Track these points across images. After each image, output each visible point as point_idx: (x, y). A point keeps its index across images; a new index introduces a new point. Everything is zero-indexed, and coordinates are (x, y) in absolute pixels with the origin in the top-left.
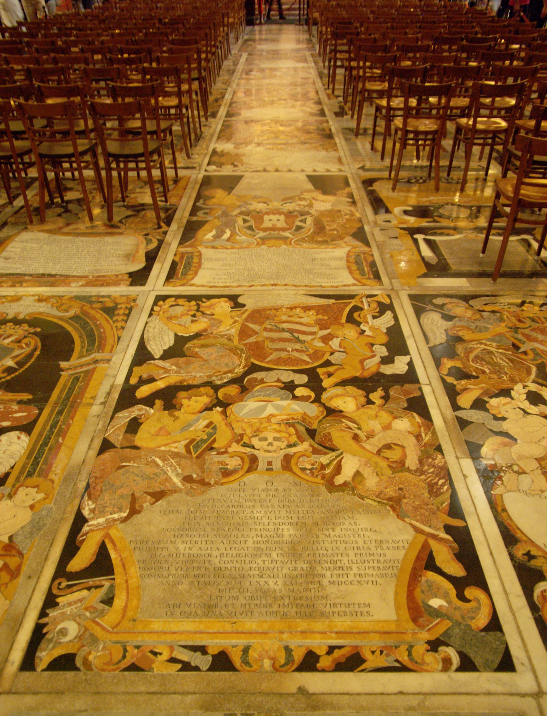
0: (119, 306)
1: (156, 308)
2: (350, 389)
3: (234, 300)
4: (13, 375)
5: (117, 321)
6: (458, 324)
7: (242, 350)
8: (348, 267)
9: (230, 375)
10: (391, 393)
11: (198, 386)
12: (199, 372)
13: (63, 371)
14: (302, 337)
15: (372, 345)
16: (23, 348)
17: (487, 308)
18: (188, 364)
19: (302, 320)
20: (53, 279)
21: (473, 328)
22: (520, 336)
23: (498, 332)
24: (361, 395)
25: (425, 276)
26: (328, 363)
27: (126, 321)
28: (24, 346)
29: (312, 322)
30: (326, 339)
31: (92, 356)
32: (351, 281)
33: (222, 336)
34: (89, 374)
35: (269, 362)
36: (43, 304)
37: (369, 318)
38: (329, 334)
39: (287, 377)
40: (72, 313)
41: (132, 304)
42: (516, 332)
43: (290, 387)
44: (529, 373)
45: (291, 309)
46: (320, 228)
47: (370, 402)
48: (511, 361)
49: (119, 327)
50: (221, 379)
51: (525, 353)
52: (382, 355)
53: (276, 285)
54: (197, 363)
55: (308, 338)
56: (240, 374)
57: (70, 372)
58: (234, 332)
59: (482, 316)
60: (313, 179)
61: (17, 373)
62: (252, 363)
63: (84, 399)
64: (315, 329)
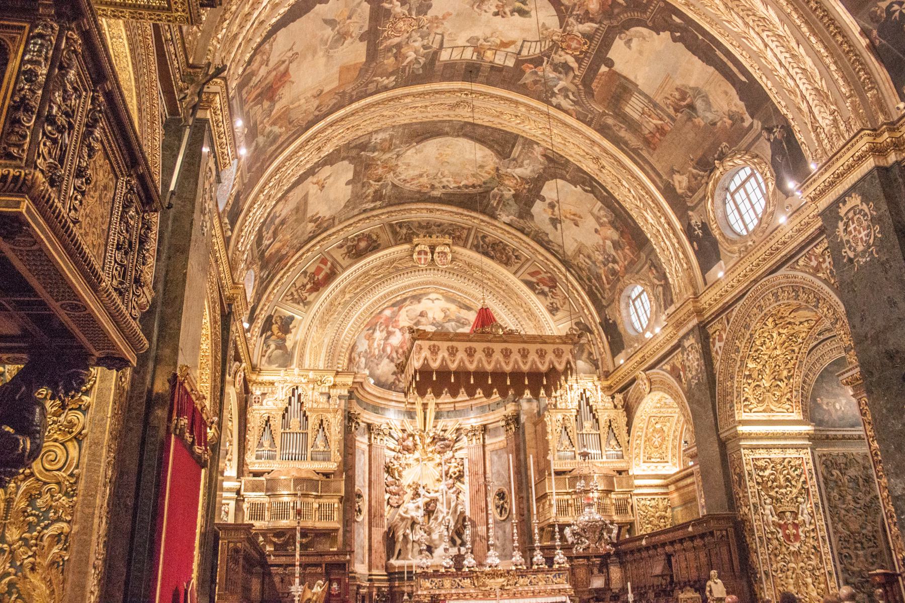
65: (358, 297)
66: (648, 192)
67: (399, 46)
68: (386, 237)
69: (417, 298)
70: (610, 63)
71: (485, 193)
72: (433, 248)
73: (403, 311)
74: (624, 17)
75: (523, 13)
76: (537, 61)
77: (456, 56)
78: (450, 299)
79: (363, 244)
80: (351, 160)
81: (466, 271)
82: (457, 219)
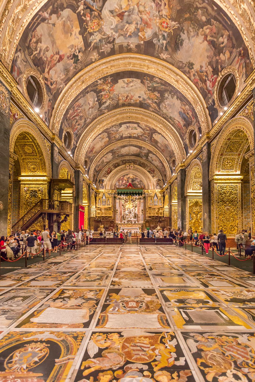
0: (79, 336)
1: (92, 337)
2: (164, 372)
3: (119, 333)
4: (37, 365)
5: (78, 342)
6: (200, 344)
7: (123, 354)
8: (159, 321)
9: (119, 365)
10: (180, 374)
11: (107, 370)
12: (108, 364)
13: (56, 363)
14: (145, 349)
15: (171, 352)
16: (42, 353)
17: (209, 337)
18: (103, 360)
19: (144, 342)
20: (56, 325)
21: (206, 345)
22: (224, 349)
23: (216, 347)
24: (169, 375)
25: (185, 325)
26: (155, 360)
27: (81, 342)
28: (43, 352)
29: (148, 343)
30: (153, 350)
31: (68, 357)
32: (160, 327)
33: (116, 348)
34: (66, 364)
35: (133, 360)
36: (52, 335)
37: (168, 341)
38: (154, 348)
39: (140, 366)
40: (62, 339)
41: (84, 335)
42: (222, 347)
43: (141, 371)
44: (231, 365)
45: (140, 337)
46: (148, 307)
47: (173, 378)
48: (223, 359)
49: (78, 344)
50: (115, 367)
51: (227, 356)
52: (175, 357)
53: (134, 328)
54: (106, 360)
55: (147, 349)
56: (122, 365)
57: (59, 364)
58: (120, 347)
59: (208, 341)
60: (144, 290)
61: (38, 364)
62: (127, 360)
63: (63, 376)
64: (149, 346)
65: (115, 176)
66: (164, 159)
67: (114, 136)
68: (121, 163)
69: (127, 175)
70: (154, 138)
71: (139, 154)
72: (130, 165)
73: (125, 177)
74: (153, 131)
75: (136, 129)
76: (141, 136)
77: (126, 135)
78: (133, 175)
79: (116, 165)
80: (111, 153)
81: (136, 170)
82: (135, 158)
